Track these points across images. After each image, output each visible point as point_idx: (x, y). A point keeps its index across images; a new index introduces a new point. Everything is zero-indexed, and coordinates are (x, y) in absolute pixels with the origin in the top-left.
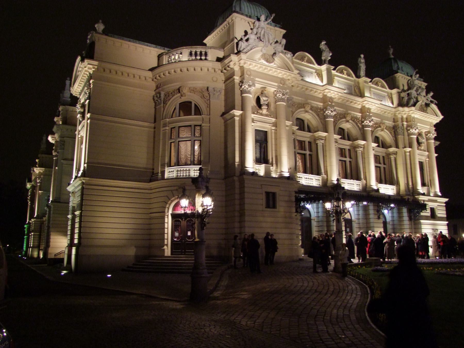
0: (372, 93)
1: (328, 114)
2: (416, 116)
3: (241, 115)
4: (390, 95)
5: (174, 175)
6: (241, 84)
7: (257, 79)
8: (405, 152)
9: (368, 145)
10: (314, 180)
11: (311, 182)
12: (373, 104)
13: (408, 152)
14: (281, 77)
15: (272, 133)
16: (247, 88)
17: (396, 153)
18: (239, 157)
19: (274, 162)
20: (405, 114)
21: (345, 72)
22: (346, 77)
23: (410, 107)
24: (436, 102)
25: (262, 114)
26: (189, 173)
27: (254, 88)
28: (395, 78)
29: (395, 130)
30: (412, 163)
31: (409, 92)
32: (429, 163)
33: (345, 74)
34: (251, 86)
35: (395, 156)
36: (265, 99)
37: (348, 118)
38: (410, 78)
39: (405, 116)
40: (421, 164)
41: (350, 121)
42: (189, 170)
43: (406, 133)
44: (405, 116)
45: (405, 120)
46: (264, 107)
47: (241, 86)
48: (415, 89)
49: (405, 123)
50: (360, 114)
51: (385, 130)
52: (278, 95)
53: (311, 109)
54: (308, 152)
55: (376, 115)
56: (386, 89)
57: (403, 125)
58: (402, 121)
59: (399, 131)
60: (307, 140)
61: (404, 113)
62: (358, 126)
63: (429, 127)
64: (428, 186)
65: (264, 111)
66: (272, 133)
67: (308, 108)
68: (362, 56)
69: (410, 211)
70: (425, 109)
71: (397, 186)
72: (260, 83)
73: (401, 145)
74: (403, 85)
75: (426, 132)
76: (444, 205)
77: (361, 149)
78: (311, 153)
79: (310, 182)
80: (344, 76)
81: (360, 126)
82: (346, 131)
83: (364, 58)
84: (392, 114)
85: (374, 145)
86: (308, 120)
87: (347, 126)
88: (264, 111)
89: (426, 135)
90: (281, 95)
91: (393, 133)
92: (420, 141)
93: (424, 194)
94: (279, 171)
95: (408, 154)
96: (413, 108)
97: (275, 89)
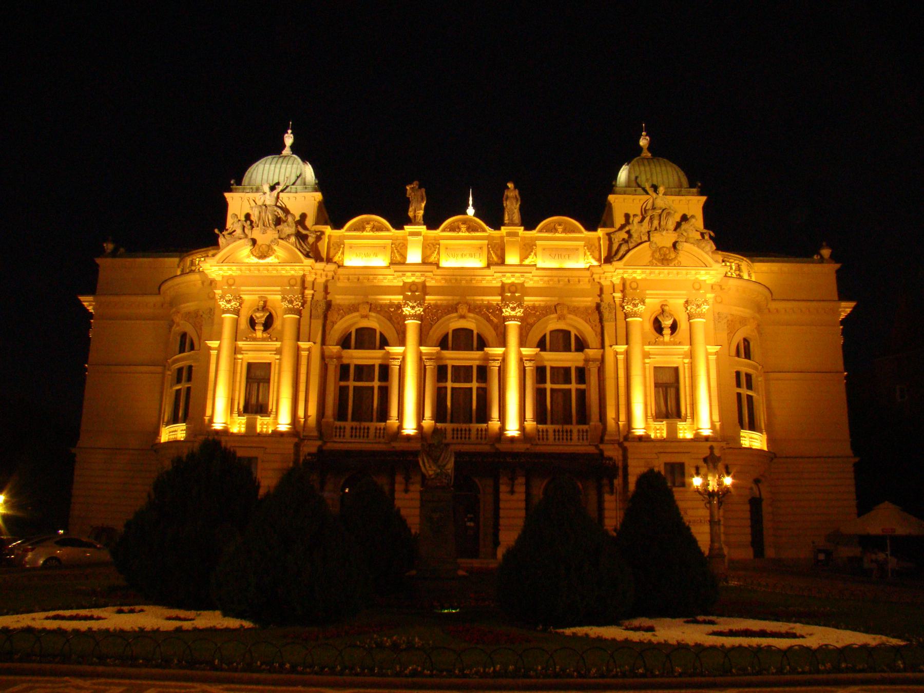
7: (243, 288)
8: (617, 353)
22: (467, 234)
24: (712, 234)
25: (255, 339)
31: (627, 229)
36: (258, 315)
43: (620, 316)
44: (617, 280)
56: (580, 232)
60: (377, 363)
63: (684, 292)
65: (259, 334)
67: (364, 310)
70: (673, 255)
72: (251, 293)
73: (607, 343)
81: (495, 320)
83: (515, 188)
95: (621, 357)
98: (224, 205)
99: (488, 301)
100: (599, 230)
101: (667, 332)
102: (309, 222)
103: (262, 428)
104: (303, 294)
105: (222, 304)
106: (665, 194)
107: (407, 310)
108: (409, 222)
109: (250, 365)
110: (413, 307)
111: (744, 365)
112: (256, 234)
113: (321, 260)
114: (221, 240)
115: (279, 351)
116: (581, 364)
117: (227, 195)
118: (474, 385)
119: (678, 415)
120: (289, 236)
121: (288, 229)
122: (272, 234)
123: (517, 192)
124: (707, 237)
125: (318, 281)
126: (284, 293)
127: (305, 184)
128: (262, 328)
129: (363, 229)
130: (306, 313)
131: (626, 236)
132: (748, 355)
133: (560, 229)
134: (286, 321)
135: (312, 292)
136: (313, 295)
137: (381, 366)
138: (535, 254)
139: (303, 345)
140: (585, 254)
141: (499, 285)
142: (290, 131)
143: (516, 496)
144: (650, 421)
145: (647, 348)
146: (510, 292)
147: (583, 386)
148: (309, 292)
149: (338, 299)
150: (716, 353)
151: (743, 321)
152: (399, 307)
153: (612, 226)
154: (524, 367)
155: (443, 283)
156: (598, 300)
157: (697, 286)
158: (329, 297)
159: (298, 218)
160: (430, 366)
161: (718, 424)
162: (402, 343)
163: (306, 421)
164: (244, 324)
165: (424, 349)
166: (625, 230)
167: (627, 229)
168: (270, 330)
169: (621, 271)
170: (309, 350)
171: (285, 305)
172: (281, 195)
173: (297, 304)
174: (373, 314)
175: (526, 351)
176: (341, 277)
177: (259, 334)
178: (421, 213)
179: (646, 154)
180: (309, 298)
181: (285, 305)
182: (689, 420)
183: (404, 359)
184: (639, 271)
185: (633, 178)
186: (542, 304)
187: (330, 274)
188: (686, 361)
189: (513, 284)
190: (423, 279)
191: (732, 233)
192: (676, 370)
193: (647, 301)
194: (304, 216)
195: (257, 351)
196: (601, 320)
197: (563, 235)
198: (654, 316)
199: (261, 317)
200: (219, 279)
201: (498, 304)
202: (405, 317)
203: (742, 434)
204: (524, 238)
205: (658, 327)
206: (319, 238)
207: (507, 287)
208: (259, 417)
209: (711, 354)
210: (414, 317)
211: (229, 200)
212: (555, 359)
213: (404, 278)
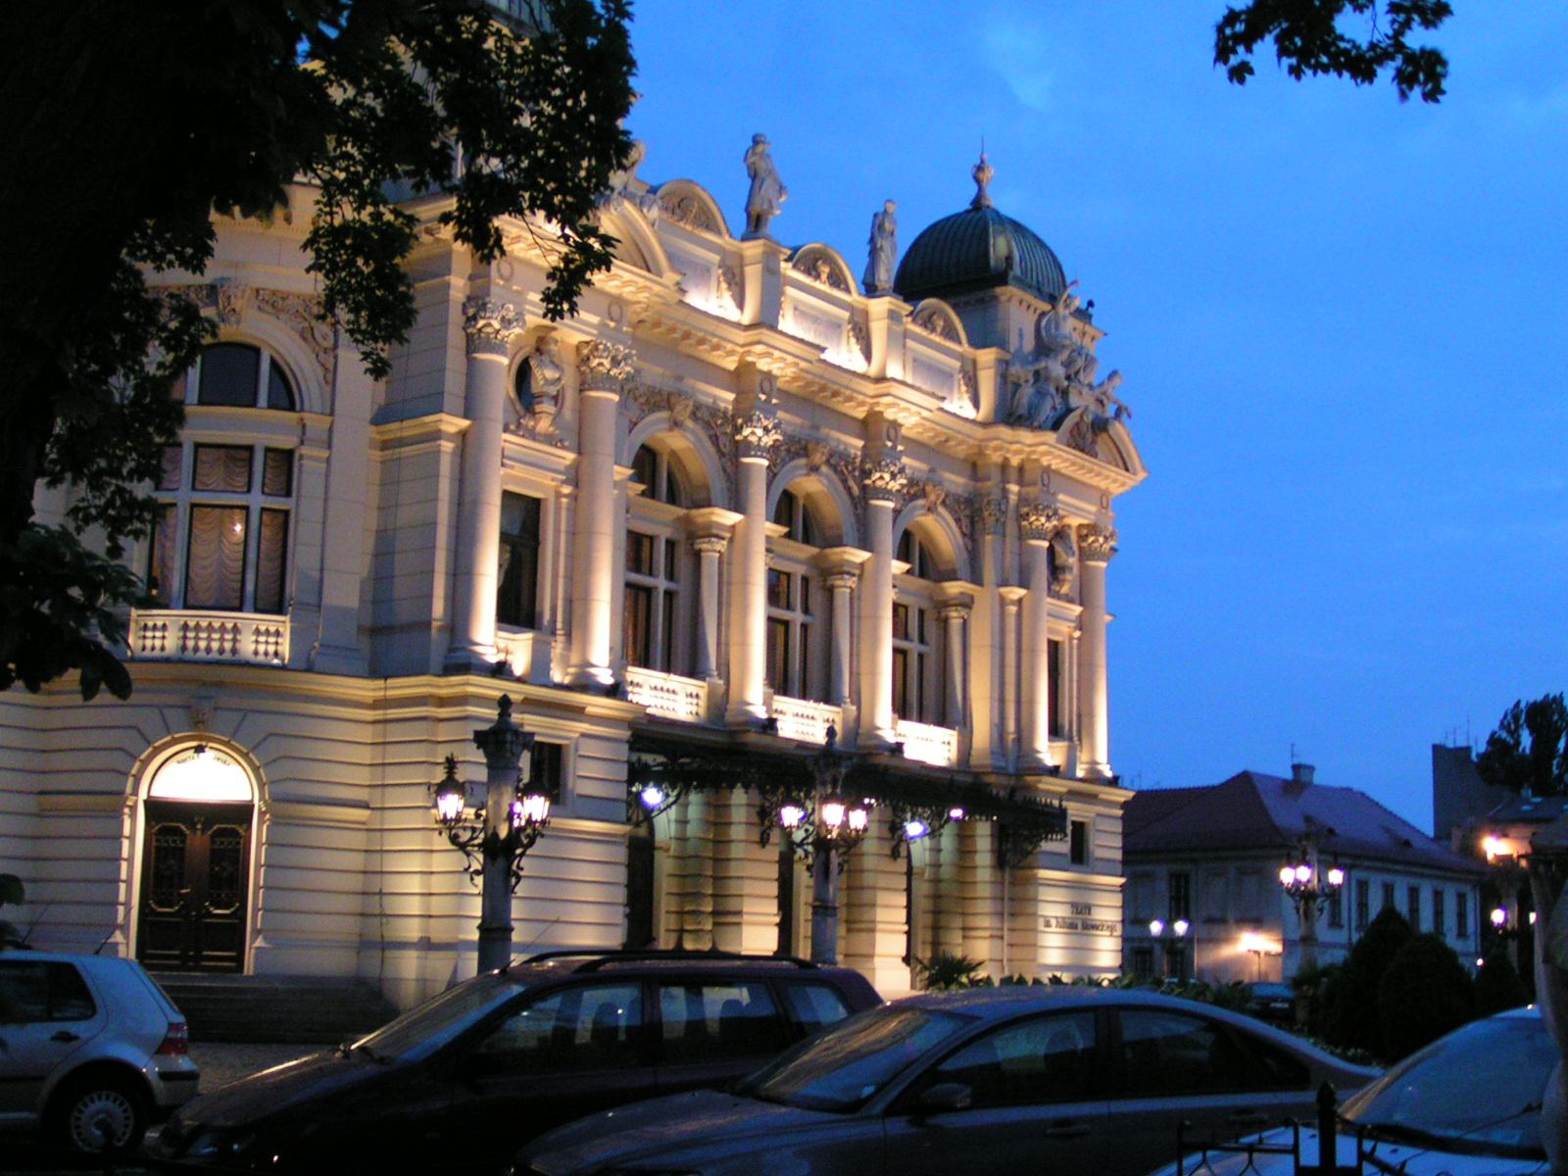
0: (909, 357)
1: (753, 439)
2: (1055, 464)
3: (463, 435)
4: (969, 368)
5: (171, 642)
6: (471, 312)
8: (1003, 602)
9: (878, 567)
10: (681, 698)
11: (671, 705)
12: (914, 409)
13: (1013, 603)
14: (614, 291)
15: (558, 508)
16: (498, 332)
17: (966, 603)
18: (446, 599)
19: (559, 625)
20: (1017, 453)
21: (825, 270)
23: (1040, 428)
25: (533, 435)
26: (235, 640)
27: (518, 331)
28: (995, 298)
29: (972, 513)
30: (1025, 646)
32: (1079, 647)
33: (824, 276)
34: (510, 322)
35: (964, 612)
36: (550, 374)
37: (818, 458)
38: (1047, 307)
39: (1015, 461)
40: (1054, 648)
41: (824, 469)
42: (236, 630)
43: (1011, 529)
44: (1015, 461)
45: (1014, 475)
46: (547, 407)
47: (475, 318)
48: (1064, 356)
49: (1014, 488)
50: (860, 443)
51: (941, 509)
52: (595, 362)
53: (694, 416)
54: (661, 583)
55: (916, 447)
57: (1005, 492)
58: (1005, 481)
61: (1015, 447)
62: (849, 489)
63: (1093, 509)
64: (1071, 739)
66: (558, 508)
69: (1001, 835)
70: (1089, 436)
71: (960, 734)
74: (1021, 335)
75: (1081, 526)
76: (1120, 812)
77: (852, 582)
78: (672, 586)
79: (666, 704)
80: (818, 285)
81: (856, 490)
82: (801, 502)
84: (971, 447)
85: (898, 567)
86: (673, 453)
87: (811, 485)
88: (544, 425)
89: (1082, 538)
90: (607, 363)
91: (965, 522)
92: (1058, 562)
93: (1054, 771)
94: (575, 659)
95: (1013, 609)
96: (1051, 437)
97: (587, 338)
99: (846, 444)
162: (737, 502)
188: (1077, 634)
210: (773, 451)
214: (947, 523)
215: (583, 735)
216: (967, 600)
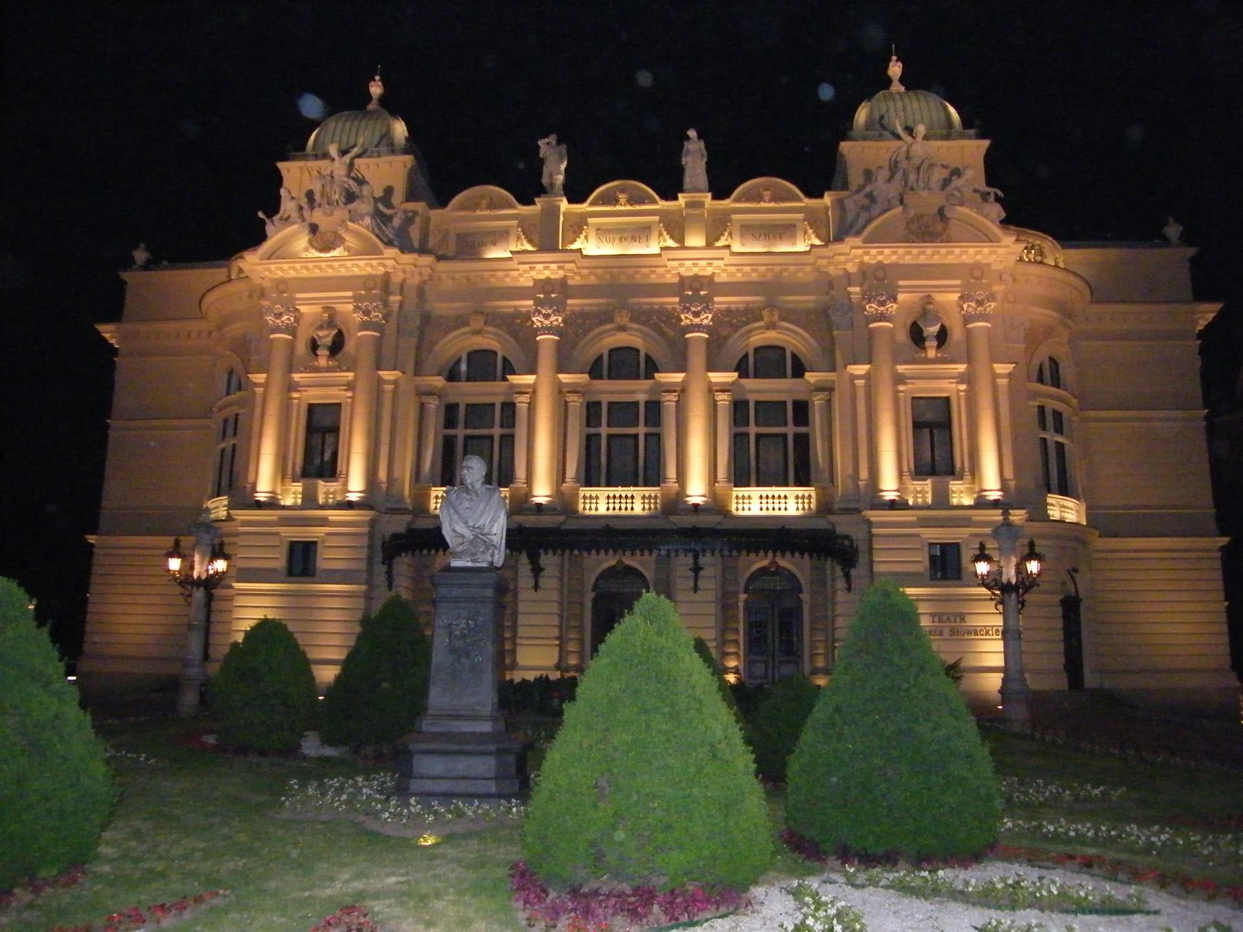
7: (298, 295)
22: (628, 208)
24: (999, 193)
25: (317, 370)
31: (868, 189)
35: (822, 395)
36: (321, 333)
39: (852, 268)
59: (836, 318)
60: (498, 401)
63: (958, 282)
65: (322, 362)
67: (478, 323)
68: (692, 133)
70: (939, 228)
77: (673, 397)
80: (623, 208)
81: (671, 333)
83: (699, 137)
95: (860, 383)
96: (857, 241)
98: (277, 180)
99: (661, 304)
100: (826, 194)
101: (931, 344)
102: (397, 198)
103: (327, 498)
104: (386, 304)
105: (270, 318)
106: (926, 138)
107: (537, 320)
108: (541, 191)
109: (312, 408)
110: (547, 316)
111: (1052, 398)
112: (317, 216)
113: (411, 250)
114: (269, 228)
115: (350, 386)
116: (800, 397)
117: (280, 165)
118: (641, 430)
119: (951, 472)
120: (362, 217)
121: (363, 207)
122: (341, 213)
123: (702, 144)
124: (992, 198)
125: (409, 281)
126: (357, 298)
127: (392, 145)
128: (327, 353)
129: (477, 206)
130: (391, 328)
131: (866, 202)
132: (1056, 382)
133: (767, 195)
134: (359, 338)
135: (399, 298)
136: (401, 304)
137: (504, 405)
138: (730, 235)
139: (386, 375)
140: (805, 232)
141: (676, 280)
142: (377, 78)
143: (699, 596)
144: (907, 478)
145: (901, 368)
146: (691, 289)
147: (803, 430)
148: (395, 299)
149: (440, 308)
150: (1009, 375)
151: (1049, 332)
152: (527, 317)
153: (845, 186)
154: (715, 403)
155: (593, 280)
156: (826, 298)
157: (976, 272)
158: (427, 307)
159: (379, 193)
160: (576, 402)
161: (1012, 484)
163: (388, 489)
164: (302, 349)
165: (564, 378)
166: (862, 194)
167: (868, 189)
168: (339, 356)
169: (860, 251)
170: (395, 383)
171: (358, 317)
172: (357, 161)
173: (377, 316)
174: (490, 329)
175: (716, 377)
176: (444, 277)
177: (322, 362)
178: (560, 179)
179: (897, 87)
180: (396, 307)
181: (358, 317)
182: (967, 477)
183: (534, 392)
184: (887, 251)
185: (877, 117)
186: (742, 307)
187: (427, 271)
188: (963, 387)
189: (696, 278)
190: (561, 273)
191: (1031, 197)
192: (948, 399)
193: (901, 297)
194: (389, 191)
195: (318, 385)
196: (830, 330)
197: (772, 205)
198: (909, 322)
199: (326, 337)
200: (266, 284)
201: (674, 309)
202: (536, 332)
203: (1049, 501)
204: (713, 212)
205: (917, 335)
206: (409, 220)
207: (687, 282)
208: (321, 483)
209: (1001, 376)
210: (549, 330)
211: (284, 173)
212: (760, 388)
213: (533, 273)
214: (788, 329)
215: (328, 534)
216: (829, 385)
